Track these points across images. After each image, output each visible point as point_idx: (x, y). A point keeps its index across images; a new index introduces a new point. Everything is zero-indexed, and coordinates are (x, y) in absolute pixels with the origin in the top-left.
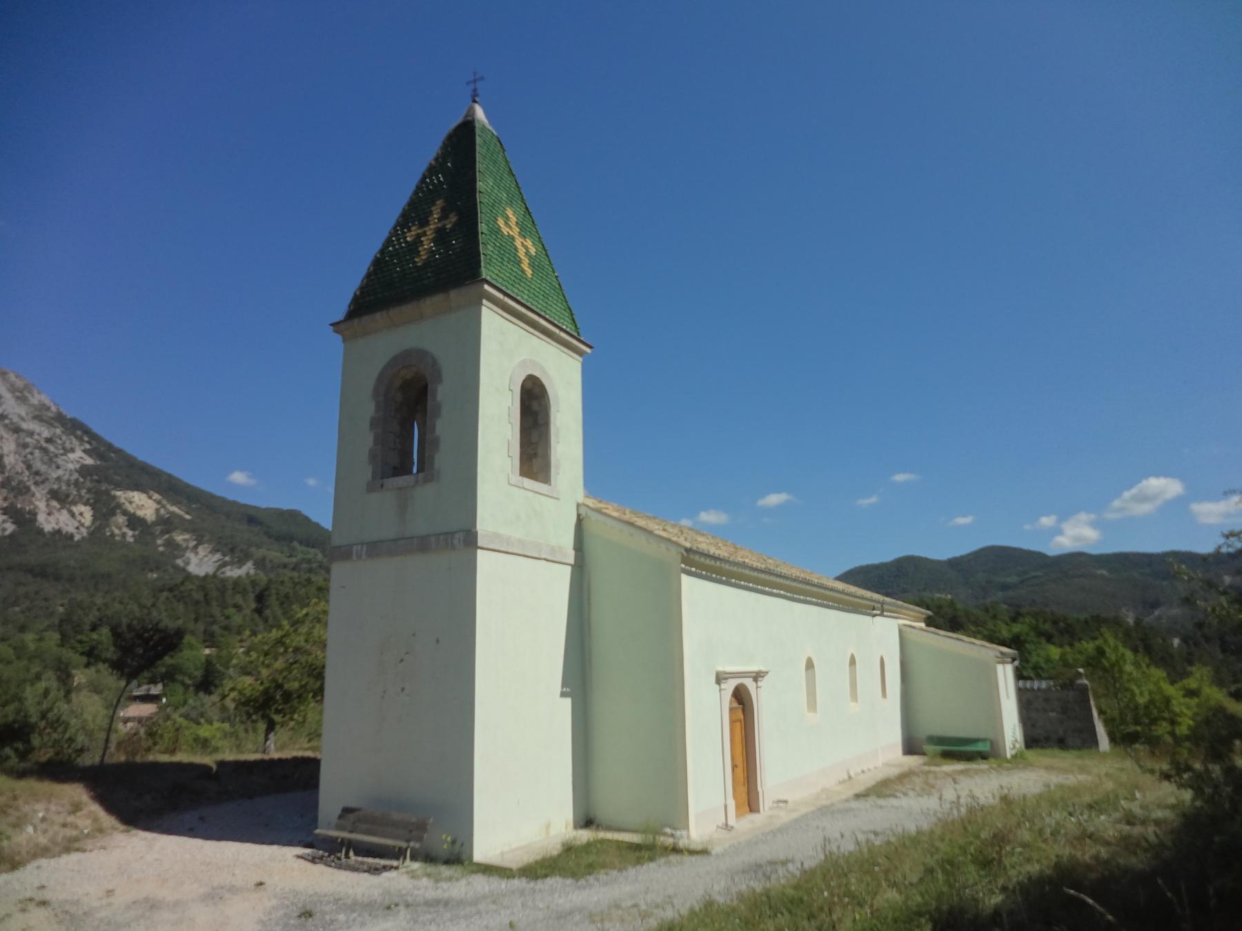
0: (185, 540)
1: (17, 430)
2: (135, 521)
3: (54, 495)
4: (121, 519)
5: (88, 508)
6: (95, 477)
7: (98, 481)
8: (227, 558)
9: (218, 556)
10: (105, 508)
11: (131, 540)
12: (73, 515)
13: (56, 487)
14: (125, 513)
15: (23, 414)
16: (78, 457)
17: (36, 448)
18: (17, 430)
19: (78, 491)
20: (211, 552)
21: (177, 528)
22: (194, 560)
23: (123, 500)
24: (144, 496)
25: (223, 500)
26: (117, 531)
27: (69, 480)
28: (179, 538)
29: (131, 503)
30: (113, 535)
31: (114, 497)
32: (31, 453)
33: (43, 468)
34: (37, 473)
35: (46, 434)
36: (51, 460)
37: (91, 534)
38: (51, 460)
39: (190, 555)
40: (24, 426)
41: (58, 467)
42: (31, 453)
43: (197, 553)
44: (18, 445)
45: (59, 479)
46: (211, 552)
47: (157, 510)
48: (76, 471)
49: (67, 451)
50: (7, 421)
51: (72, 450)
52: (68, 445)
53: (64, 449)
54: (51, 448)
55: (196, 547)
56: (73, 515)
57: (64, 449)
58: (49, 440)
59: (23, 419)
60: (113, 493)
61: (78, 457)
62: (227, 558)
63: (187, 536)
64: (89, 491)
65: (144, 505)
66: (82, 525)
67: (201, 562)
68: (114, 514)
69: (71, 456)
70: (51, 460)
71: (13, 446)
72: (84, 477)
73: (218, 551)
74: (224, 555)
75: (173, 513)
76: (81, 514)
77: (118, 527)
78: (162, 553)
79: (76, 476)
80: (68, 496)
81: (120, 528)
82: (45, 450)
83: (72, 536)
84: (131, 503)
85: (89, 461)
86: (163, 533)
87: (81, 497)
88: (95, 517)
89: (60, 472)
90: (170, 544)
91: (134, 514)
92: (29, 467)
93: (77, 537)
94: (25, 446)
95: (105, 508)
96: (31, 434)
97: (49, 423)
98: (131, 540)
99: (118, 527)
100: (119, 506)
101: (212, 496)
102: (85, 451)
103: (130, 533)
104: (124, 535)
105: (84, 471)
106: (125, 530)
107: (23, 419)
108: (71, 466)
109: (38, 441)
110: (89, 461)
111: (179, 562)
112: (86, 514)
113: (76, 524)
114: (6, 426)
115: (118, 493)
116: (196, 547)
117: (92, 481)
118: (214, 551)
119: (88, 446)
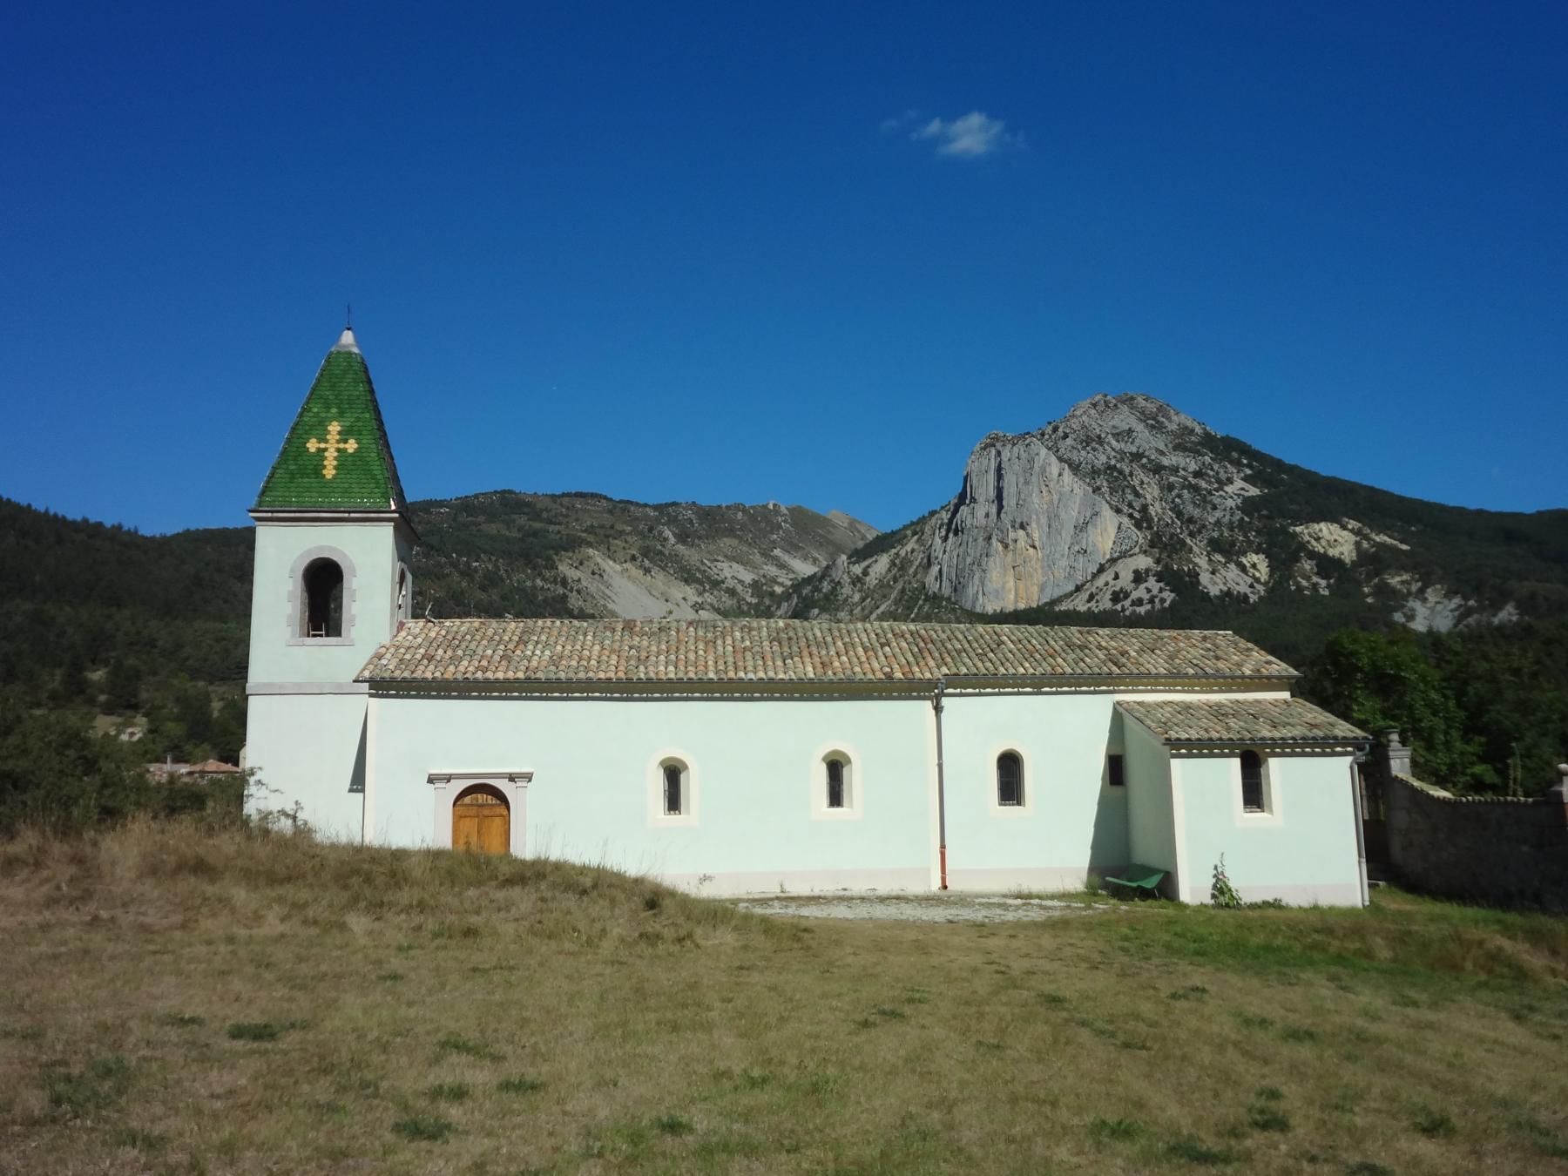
0: (1403, 582)
1: (1157, 469)
2: (1327, 565)
3: (1215, 546)
4: (1308, 565)
5: (1262, 556)
6: (1265, 512)
7: (1269, 517)
8: (1471, 603)
9: (1457, 601)
10: (1285, 553)
11: (1326, 593)
12: (1243, 569)
13: (1216, 534)
14: (1312, 555)
15: (1162, 447)
16: (1239, 488)
17: (1183, 487)
18: (1157, 469)
19: (1245, 536)
20: (1445, 596)
21: (1389, 566)
22: (1421, 610)
23: (1307, 538)
24: (1335, 527)
25: (1461, 511)
26: (1304, 583)
27: (1231, 523)
28: (1395, 581)
29: (1318, 539)
30: (1300, 589)
31: (1295, 535)
32: (1179, 496)
33: (1196, 513)
34: (1191, 520)
35: (1193, 467)
36: (1204, 500)
37: (1271, 591)
38: (1204, 500)
39: (1415, 604)
40: (1165, 462)
41: (1215, 508)
42: (1179, 496)
43: (1425, 600)
44: (1162, 489)
45: (1218, 523)
46: (1445, 596)
47: (1358, 544)
48: (1238, 508)
49: (1222, 484)
50: (1144, 461)
51: (1230, 481)
52: (1223, 476)
53: (1219, 481)
54: (1203, 484)
55: (1422, 591)
56: (1243, 569)
57: (1219, 481)
58: (1197, 474)
59: (1162, 453)
60: (1291, 529)
61: (1239, 488)
62: (1471, 603)
63: (1406, 577)
64: (1259, 532)
65: (1336, 539)
66: (1257, 580)
67: (1432, 613)
68: (1298, 560)
69: (1229, 489)
70: (1204, 500)
71: (1156, 492)
72: (1250, 515)
73: (1456, 593)
74: (1466, 598)
75: (1383, 545)
76: (1254, 566)
77: (1306, 575)
78: (1370, 607)
79: (1238, 515)
80: (1233, 544)
81: (1308, 578)
82: (1195, 489)
83: (1246, 597)
84: (1318, 539)
85: (1254, 491)
86: (1369, 577)
87: (1250, 542)
88: (1272, 568)
89: (1218, 514)
90: (1384, 591)
91: (1325, 555)
92: (1179, 514)
93: (1253, 598)
94: (1171, 487)
95: (1285, 553)
96: (1174, 470)
97: (1195, 452)
98: (1326, 593)
99: (1306, 575)
100: (1303, 546)
101: (1442, 508)
102: (1245, 479)
103: (1323, 583)
104: (1315, 586)
105: (1248, 505)
106: (1315, 579)
107: (1162, 453)
108: (1230, 503)
109: (1185, 479)
110: (1254, 491)
111: (1398, 617)
112: (1259, 563)
113: (1250, 581)
114: (1143, 466)
115: (1298, 529)
116: (1422, 591)
117: (1260, 518)
118: (1449, 595)
119: (1249, 472)
